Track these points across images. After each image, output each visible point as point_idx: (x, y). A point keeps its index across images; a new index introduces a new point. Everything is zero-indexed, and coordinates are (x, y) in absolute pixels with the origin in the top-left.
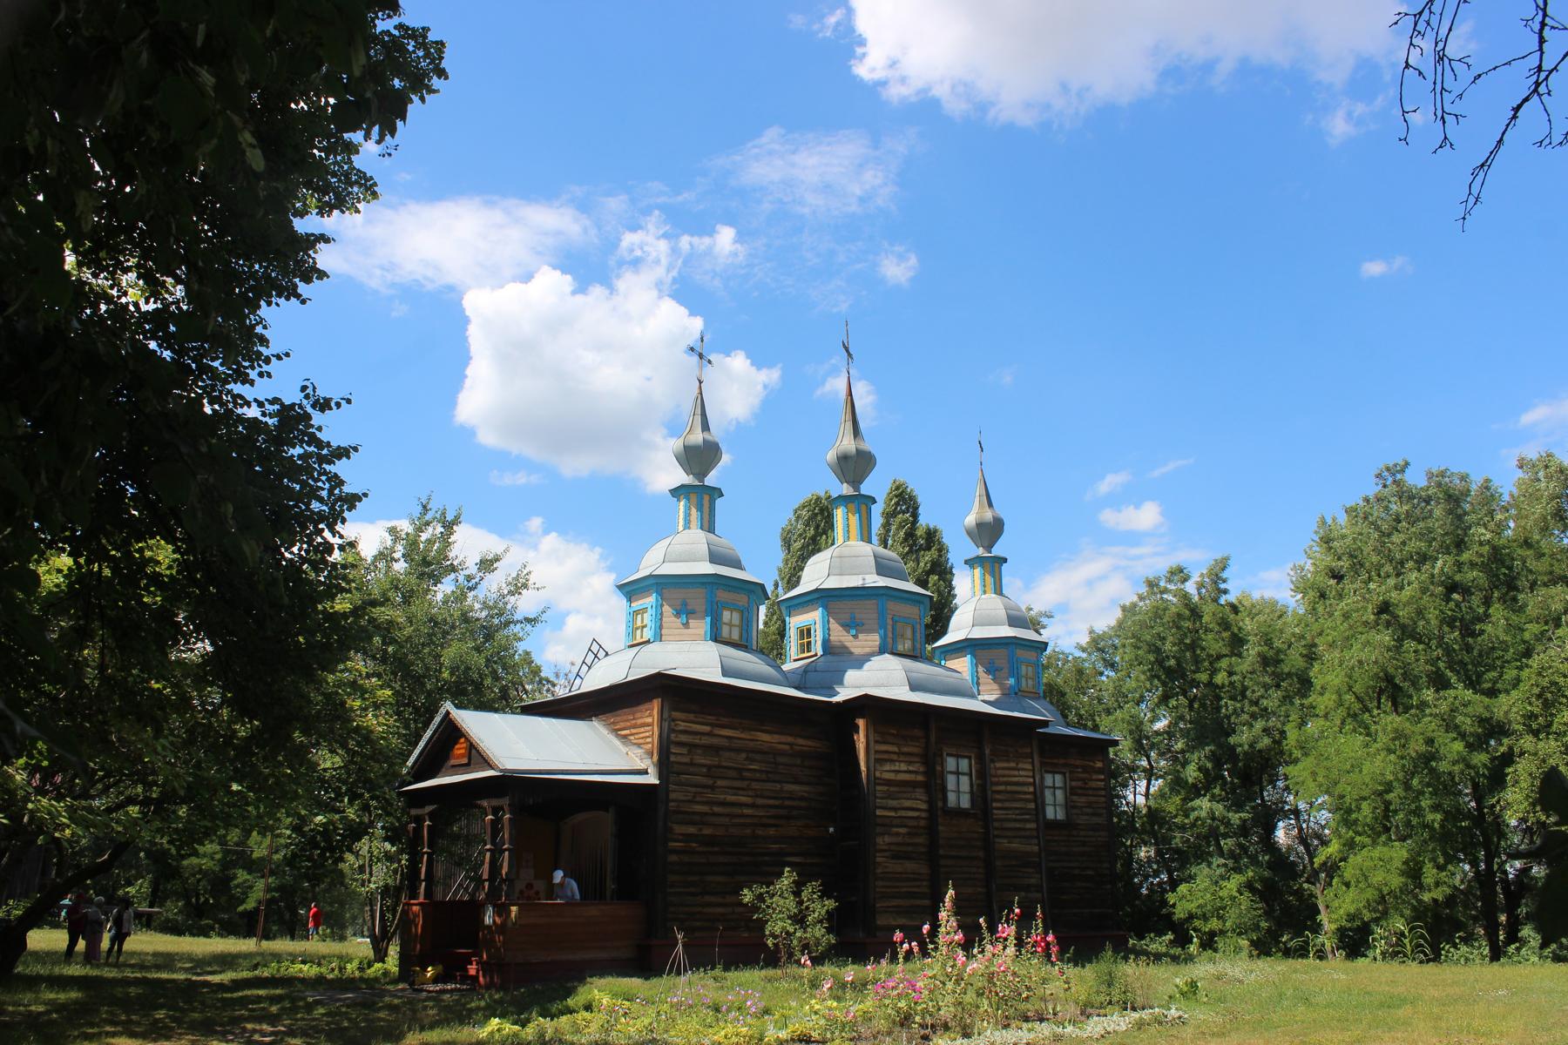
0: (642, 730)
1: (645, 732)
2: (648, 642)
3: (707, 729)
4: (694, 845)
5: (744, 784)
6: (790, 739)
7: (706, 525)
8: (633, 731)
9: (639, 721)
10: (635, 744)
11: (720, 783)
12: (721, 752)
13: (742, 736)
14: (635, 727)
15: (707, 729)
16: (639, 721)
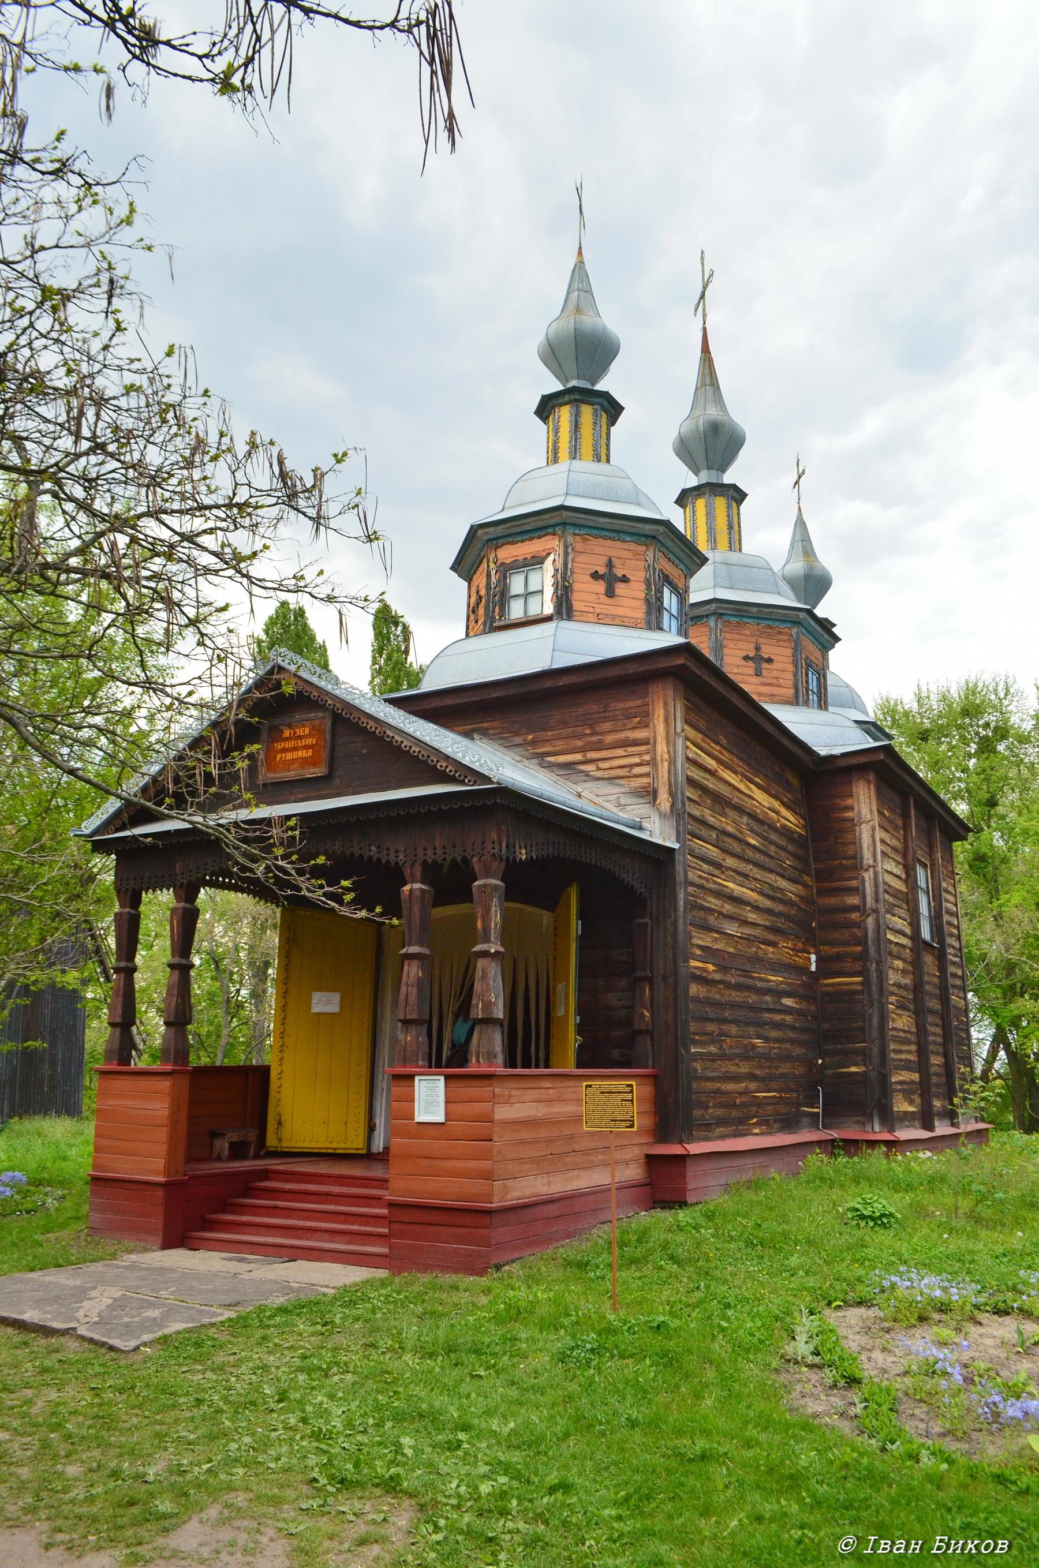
0: (620, 752)
1: (621, 758)
2: (548, 619)
3: (711, 763)
4: (711, 967)
5: (747, 868)
6: (777, 805)
7: (604, 458)
8: (591, 755)
9: (610, 738)
10: (599, 779)
11: (730, 862)
12: (727, 810)
13: (741, 786)
14: (599, 747)
15: (711, 763)
16: (610, 738)
